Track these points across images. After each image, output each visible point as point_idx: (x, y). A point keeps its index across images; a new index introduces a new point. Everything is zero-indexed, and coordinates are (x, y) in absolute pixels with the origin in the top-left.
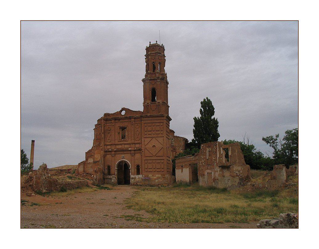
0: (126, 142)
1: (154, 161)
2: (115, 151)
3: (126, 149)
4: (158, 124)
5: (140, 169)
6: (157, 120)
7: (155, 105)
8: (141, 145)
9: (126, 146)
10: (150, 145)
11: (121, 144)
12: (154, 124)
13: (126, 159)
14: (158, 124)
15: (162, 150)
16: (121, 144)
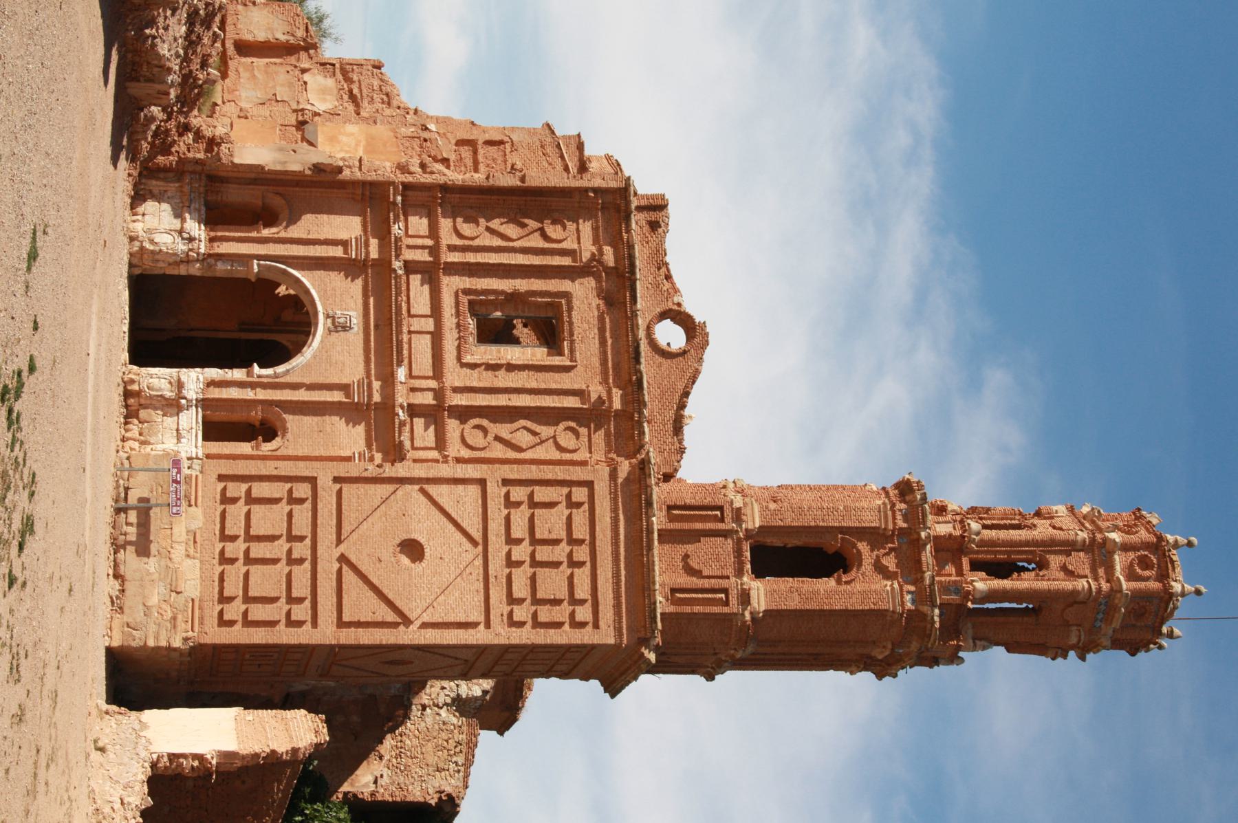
0: (450, 346)
1: (307, 554)
2: (383, 265)
3: (400, 343)
4: (583, 591)
5: (245, 448)
6: (616, 575)
7: (729, 571)
8: (434, 454)
9: (422, 347)
10: (423, 523)
11: (436, 311)
12: (582, 554)
13: (332, 353)
14: (583, 591)
15: (391, 617)
16: (436, 311)
